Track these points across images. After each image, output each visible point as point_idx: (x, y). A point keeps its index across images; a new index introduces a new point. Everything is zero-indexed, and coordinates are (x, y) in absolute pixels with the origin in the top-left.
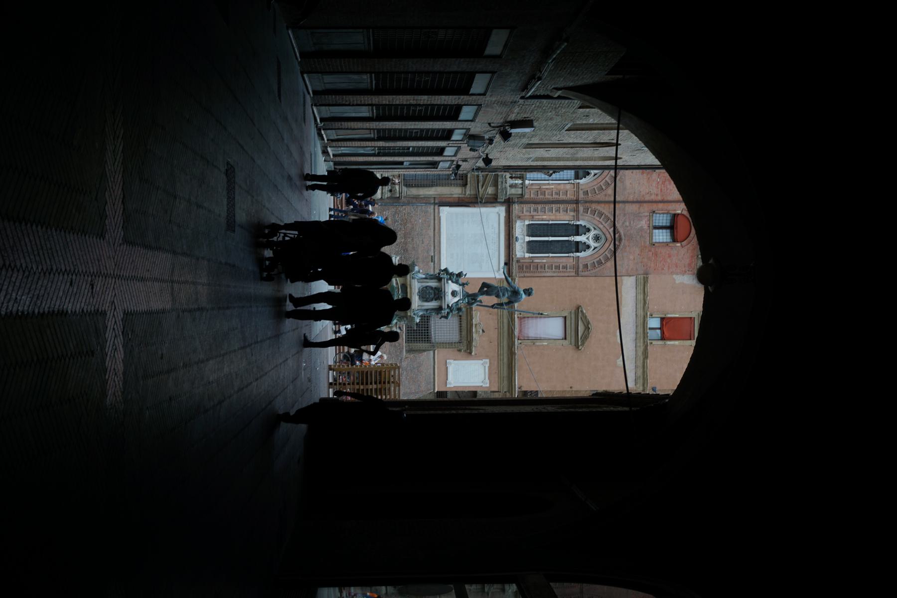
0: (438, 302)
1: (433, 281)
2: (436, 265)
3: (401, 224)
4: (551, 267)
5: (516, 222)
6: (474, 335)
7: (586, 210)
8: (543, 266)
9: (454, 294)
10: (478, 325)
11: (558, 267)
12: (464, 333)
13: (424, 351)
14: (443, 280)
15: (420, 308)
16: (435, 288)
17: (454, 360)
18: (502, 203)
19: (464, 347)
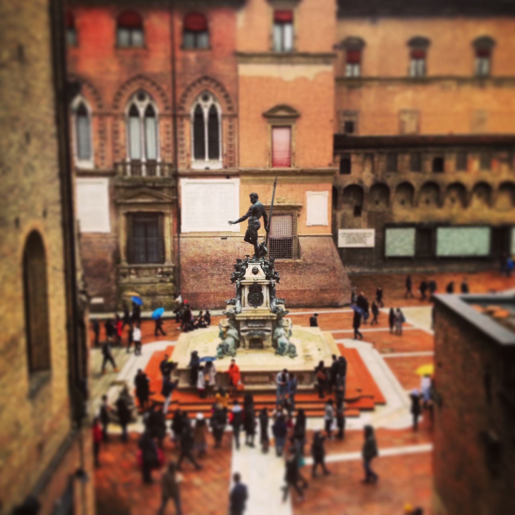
0: (263, 288)
1: (243, 292)
2: (229, 235)
3: (196, 266)
4: (231, 139)
5: (193, 170)
6: (287, 204)
7: (182, 109)
8: (231, 146)
9: (255, 272)
10: (279, 201)
11: (231, 133)
12: (285, 212)
13: (299, 244)
14: (242, 284)
15: (269, 305)
16: (250, 291)
17: (306, 219)
18: (177, 181)
19: (297, 212)
